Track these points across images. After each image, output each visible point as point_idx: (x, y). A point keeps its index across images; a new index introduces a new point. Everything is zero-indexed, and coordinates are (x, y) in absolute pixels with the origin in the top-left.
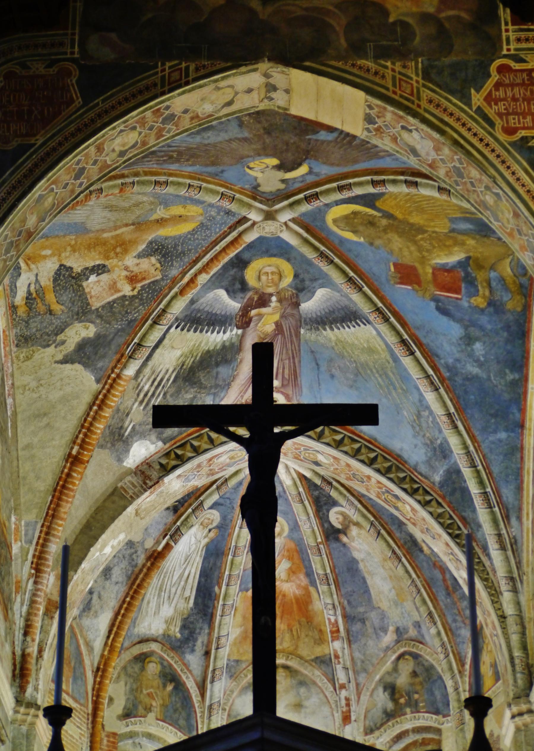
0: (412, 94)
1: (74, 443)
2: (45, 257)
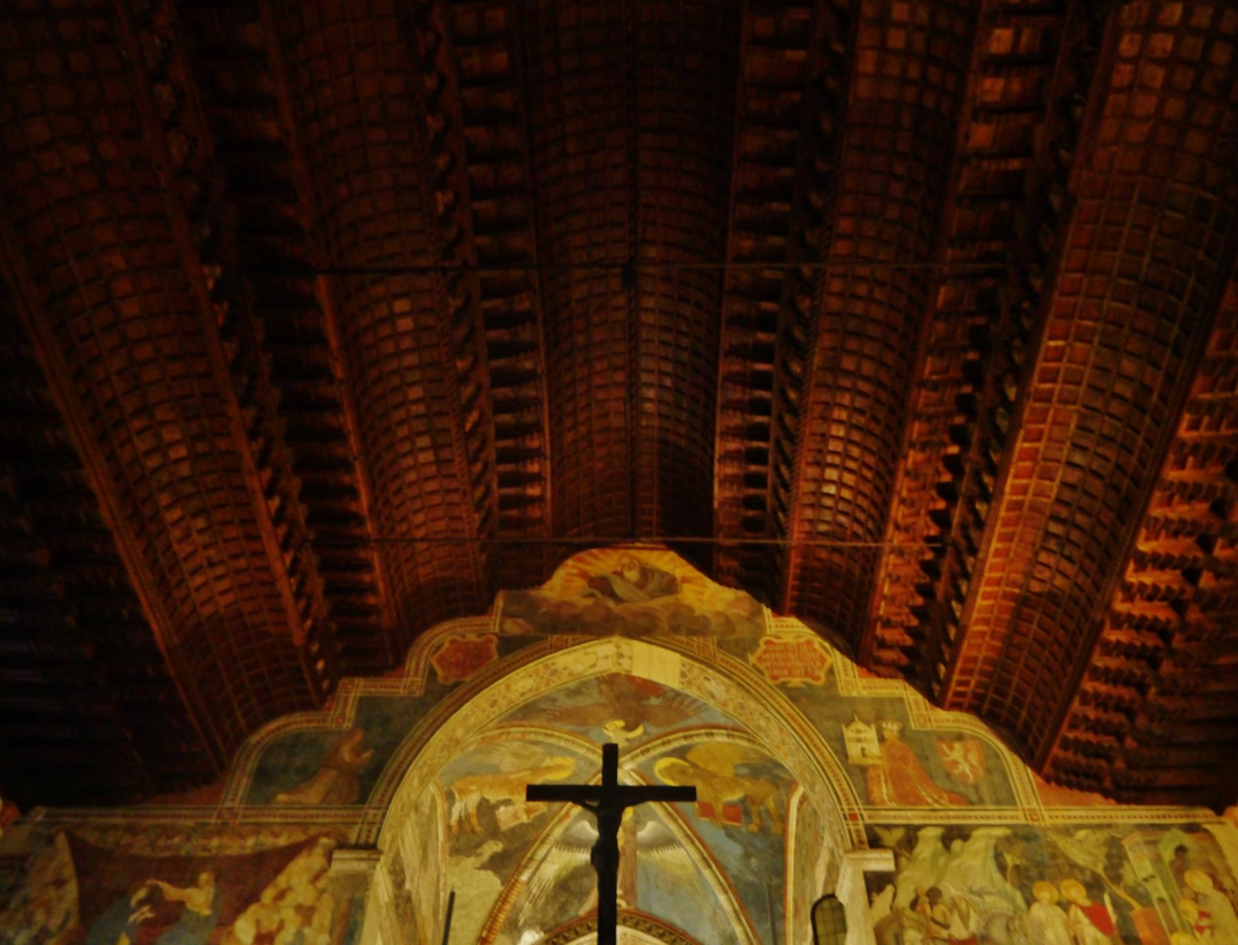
0: (710, 655)
1: (484, 928)
2: (471, 791)
